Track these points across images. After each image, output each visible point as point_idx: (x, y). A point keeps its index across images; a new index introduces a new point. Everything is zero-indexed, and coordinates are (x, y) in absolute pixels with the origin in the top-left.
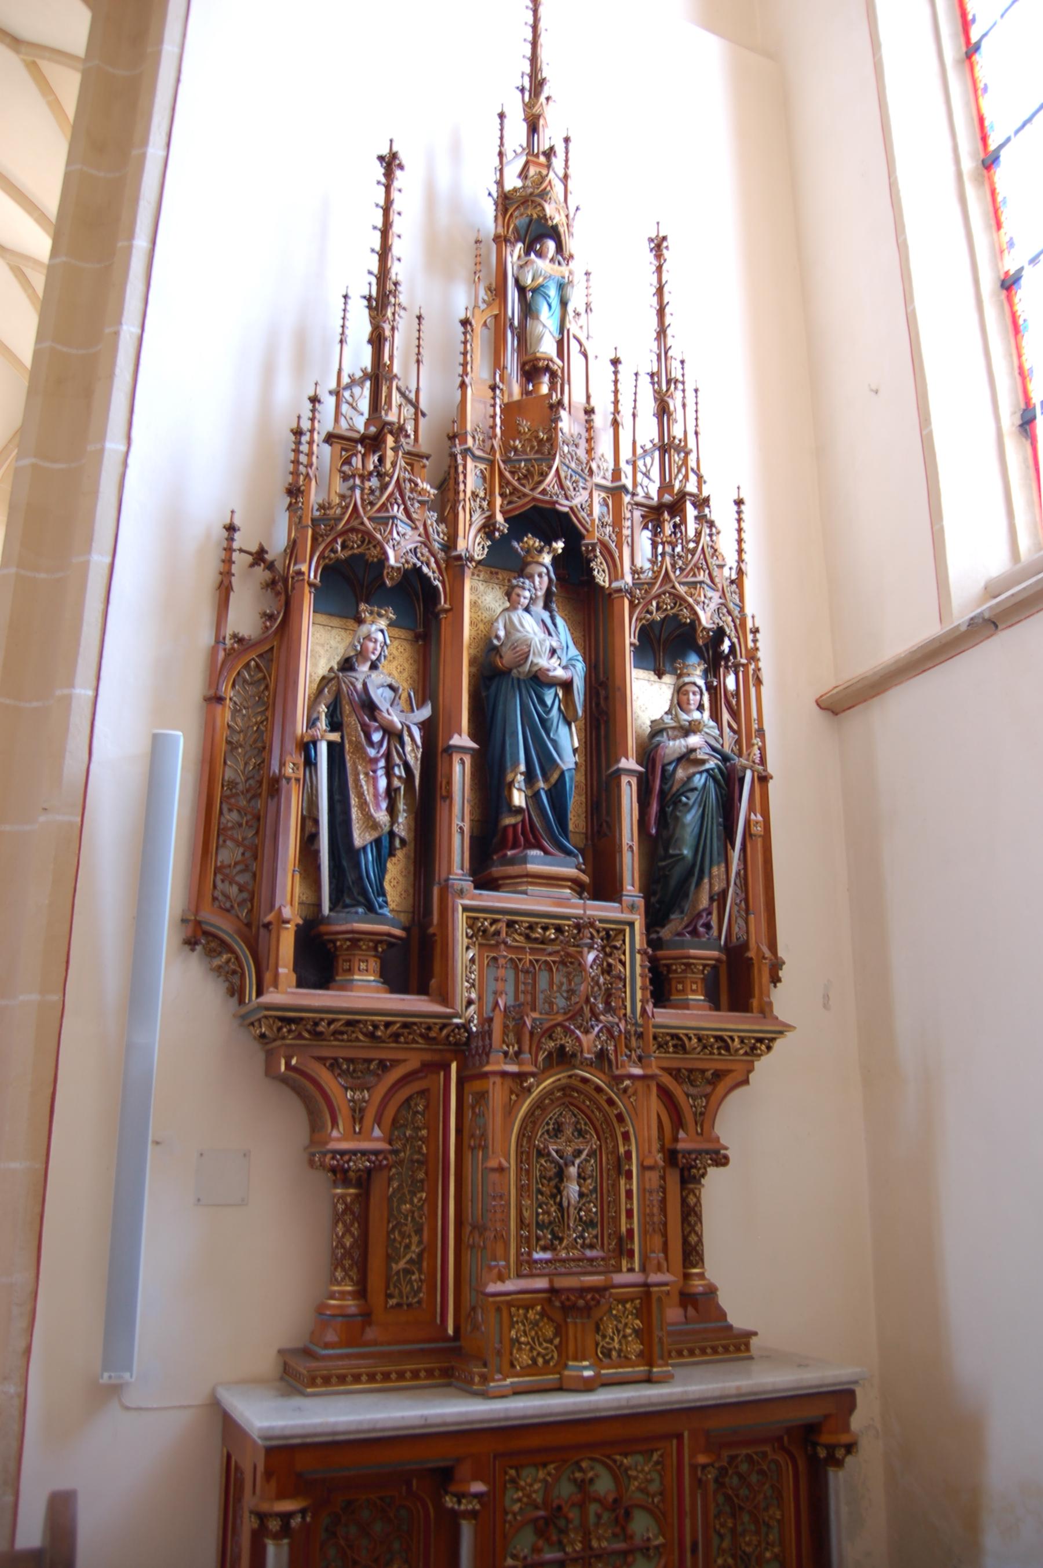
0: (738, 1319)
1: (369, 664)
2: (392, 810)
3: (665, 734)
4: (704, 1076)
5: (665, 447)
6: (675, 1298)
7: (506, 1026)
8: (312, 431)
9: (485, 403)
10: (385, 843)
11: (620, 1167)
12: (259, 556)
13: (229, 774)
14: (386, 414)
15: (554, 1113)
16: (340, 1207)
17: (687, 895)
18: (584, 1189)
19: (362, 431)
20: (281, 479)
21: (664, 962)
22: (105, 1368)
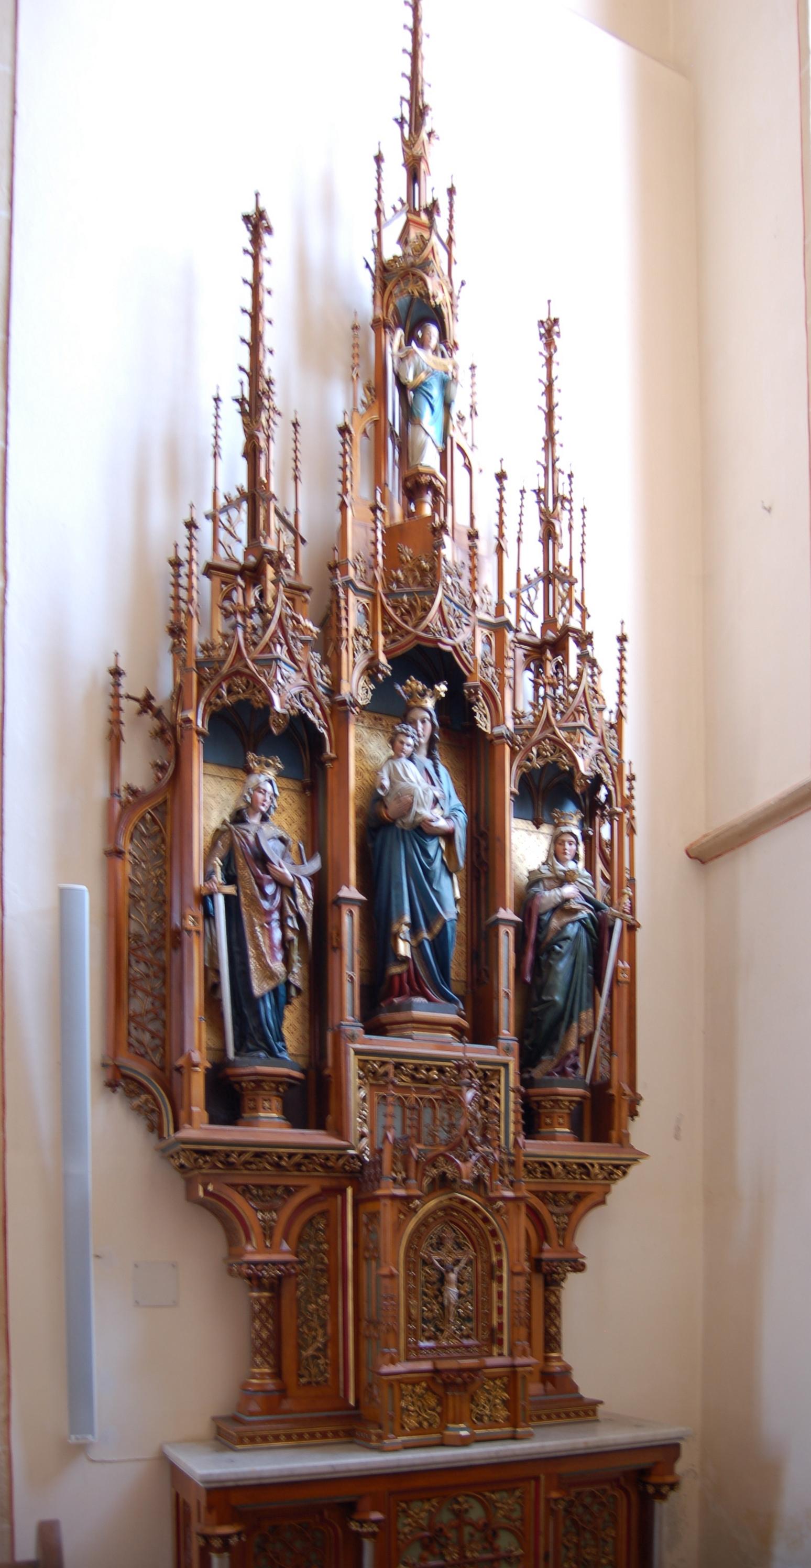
0: (587, 1391)
1: (259, 816)
2: (287, 961)
3: (541, 885)
4: (566, 1199)
5: (552, 576)
6: (537, 1376)
7: (394, 1156)
8: (190, 562)
9: (366, 527)
10: (282, 992)
11: (493, 1273)
12: (146, 703)
13: (134, 928)
14: (265, 542)
15: (437, 1229)
16: (257, 1307)
17: (556, 1039)
18: (462, 1292)
19: (241, 559)
20: (162, 618)
21: (535, 1099)
22: (72, 1433)
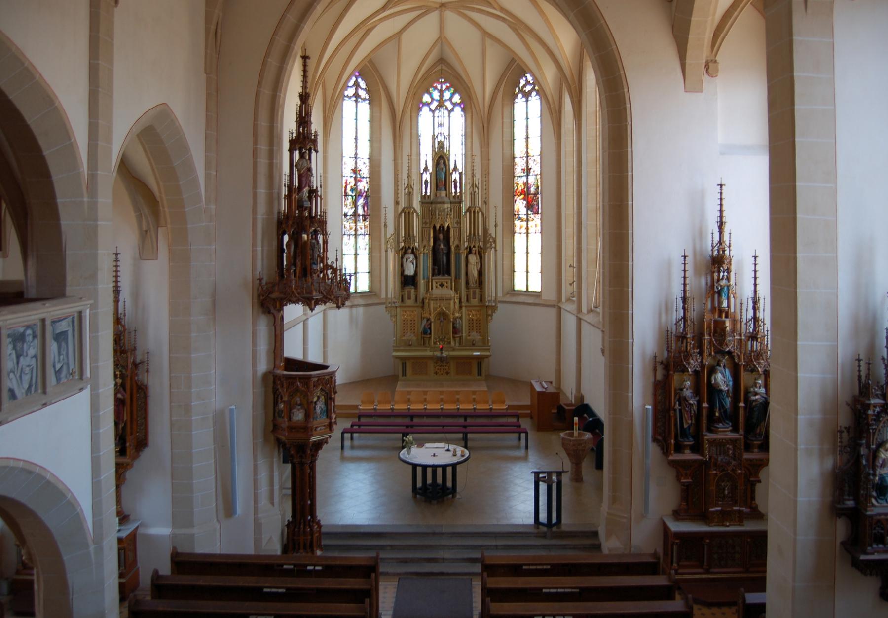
12: (662, 363)
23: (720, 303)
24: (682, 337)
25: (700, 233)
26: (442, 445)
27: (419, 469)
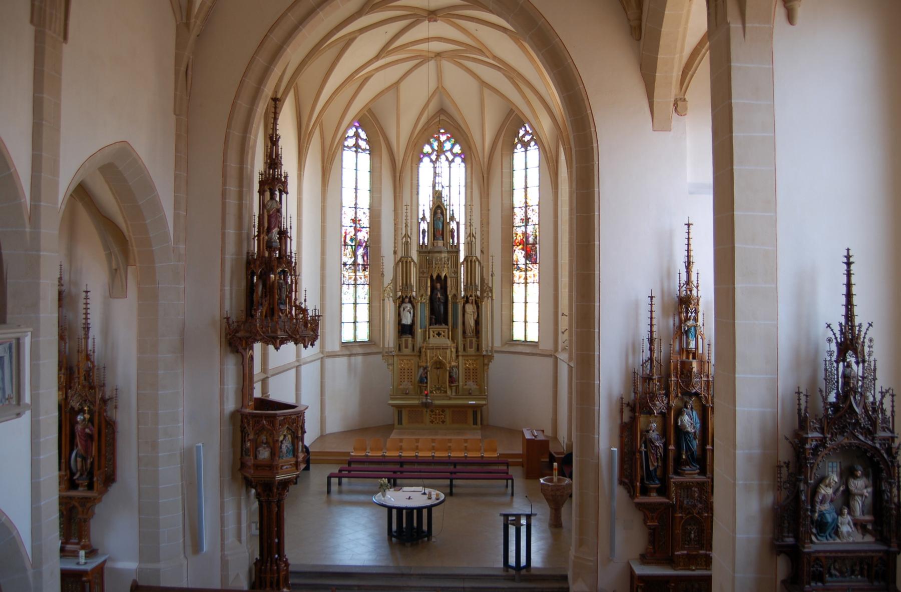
12: (628, 405)
23: (688, 344)
24: (648, 379)
25: (669, 275)
26: (420, 488)
27: (394, 512)
